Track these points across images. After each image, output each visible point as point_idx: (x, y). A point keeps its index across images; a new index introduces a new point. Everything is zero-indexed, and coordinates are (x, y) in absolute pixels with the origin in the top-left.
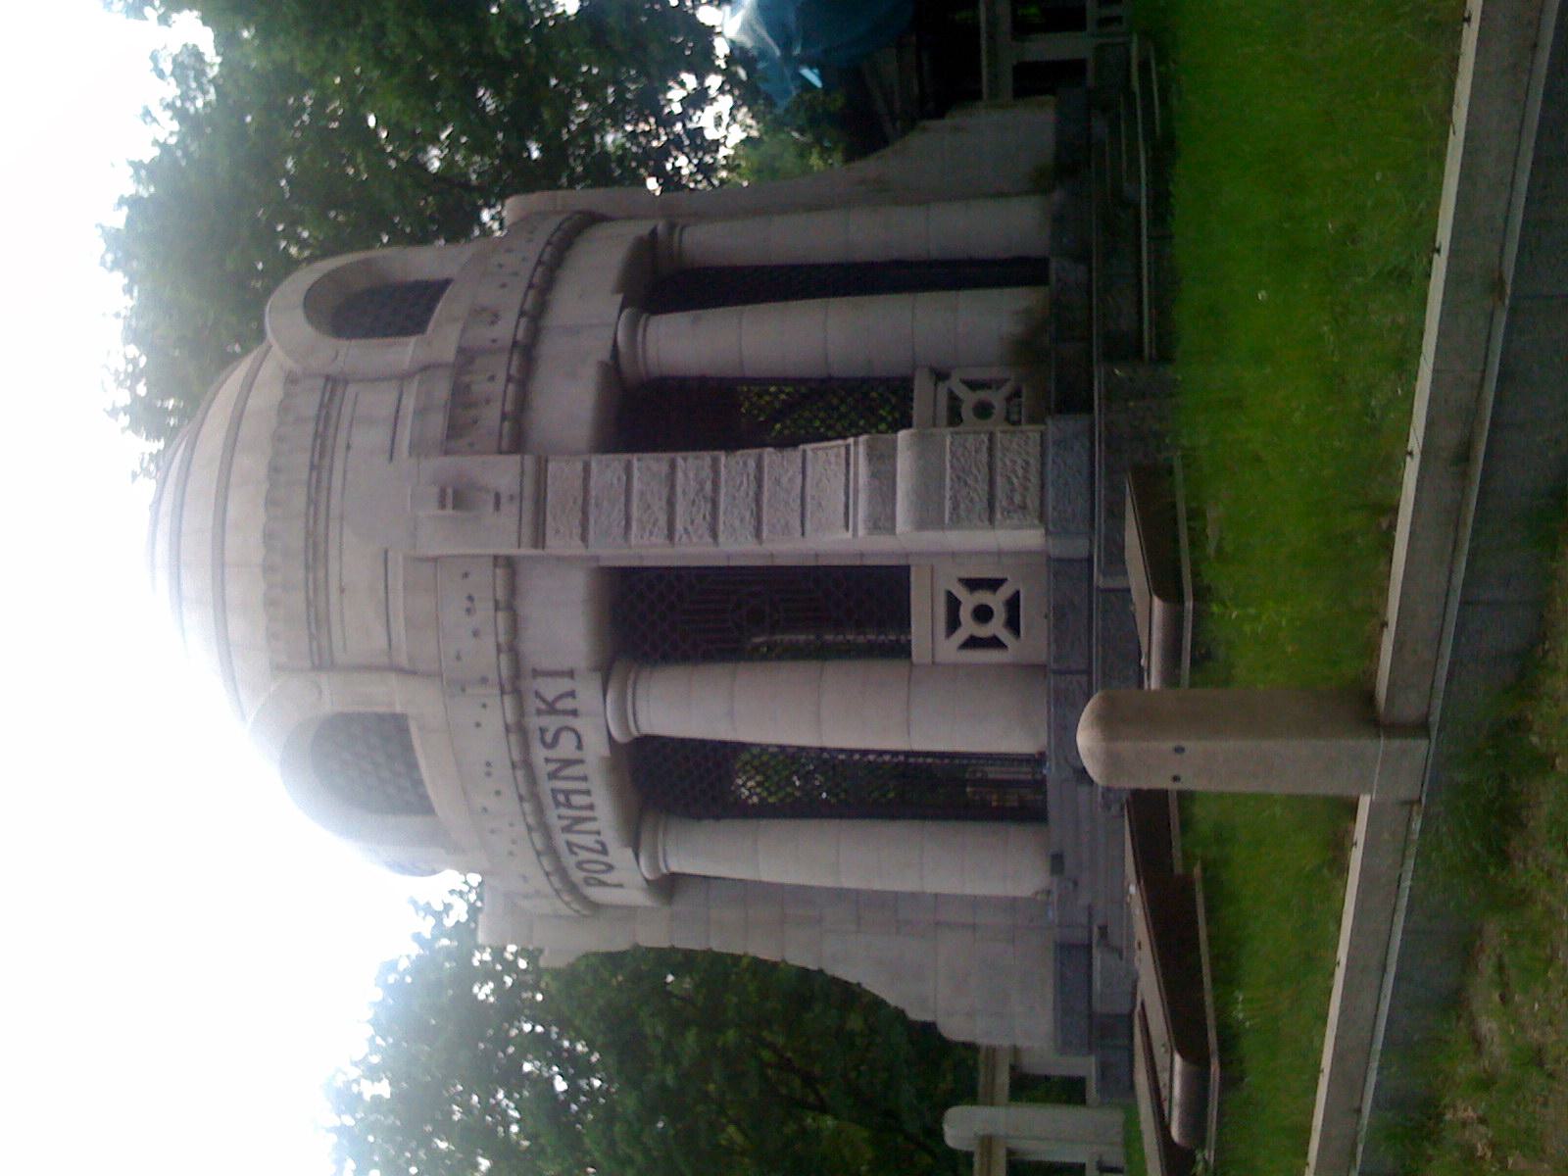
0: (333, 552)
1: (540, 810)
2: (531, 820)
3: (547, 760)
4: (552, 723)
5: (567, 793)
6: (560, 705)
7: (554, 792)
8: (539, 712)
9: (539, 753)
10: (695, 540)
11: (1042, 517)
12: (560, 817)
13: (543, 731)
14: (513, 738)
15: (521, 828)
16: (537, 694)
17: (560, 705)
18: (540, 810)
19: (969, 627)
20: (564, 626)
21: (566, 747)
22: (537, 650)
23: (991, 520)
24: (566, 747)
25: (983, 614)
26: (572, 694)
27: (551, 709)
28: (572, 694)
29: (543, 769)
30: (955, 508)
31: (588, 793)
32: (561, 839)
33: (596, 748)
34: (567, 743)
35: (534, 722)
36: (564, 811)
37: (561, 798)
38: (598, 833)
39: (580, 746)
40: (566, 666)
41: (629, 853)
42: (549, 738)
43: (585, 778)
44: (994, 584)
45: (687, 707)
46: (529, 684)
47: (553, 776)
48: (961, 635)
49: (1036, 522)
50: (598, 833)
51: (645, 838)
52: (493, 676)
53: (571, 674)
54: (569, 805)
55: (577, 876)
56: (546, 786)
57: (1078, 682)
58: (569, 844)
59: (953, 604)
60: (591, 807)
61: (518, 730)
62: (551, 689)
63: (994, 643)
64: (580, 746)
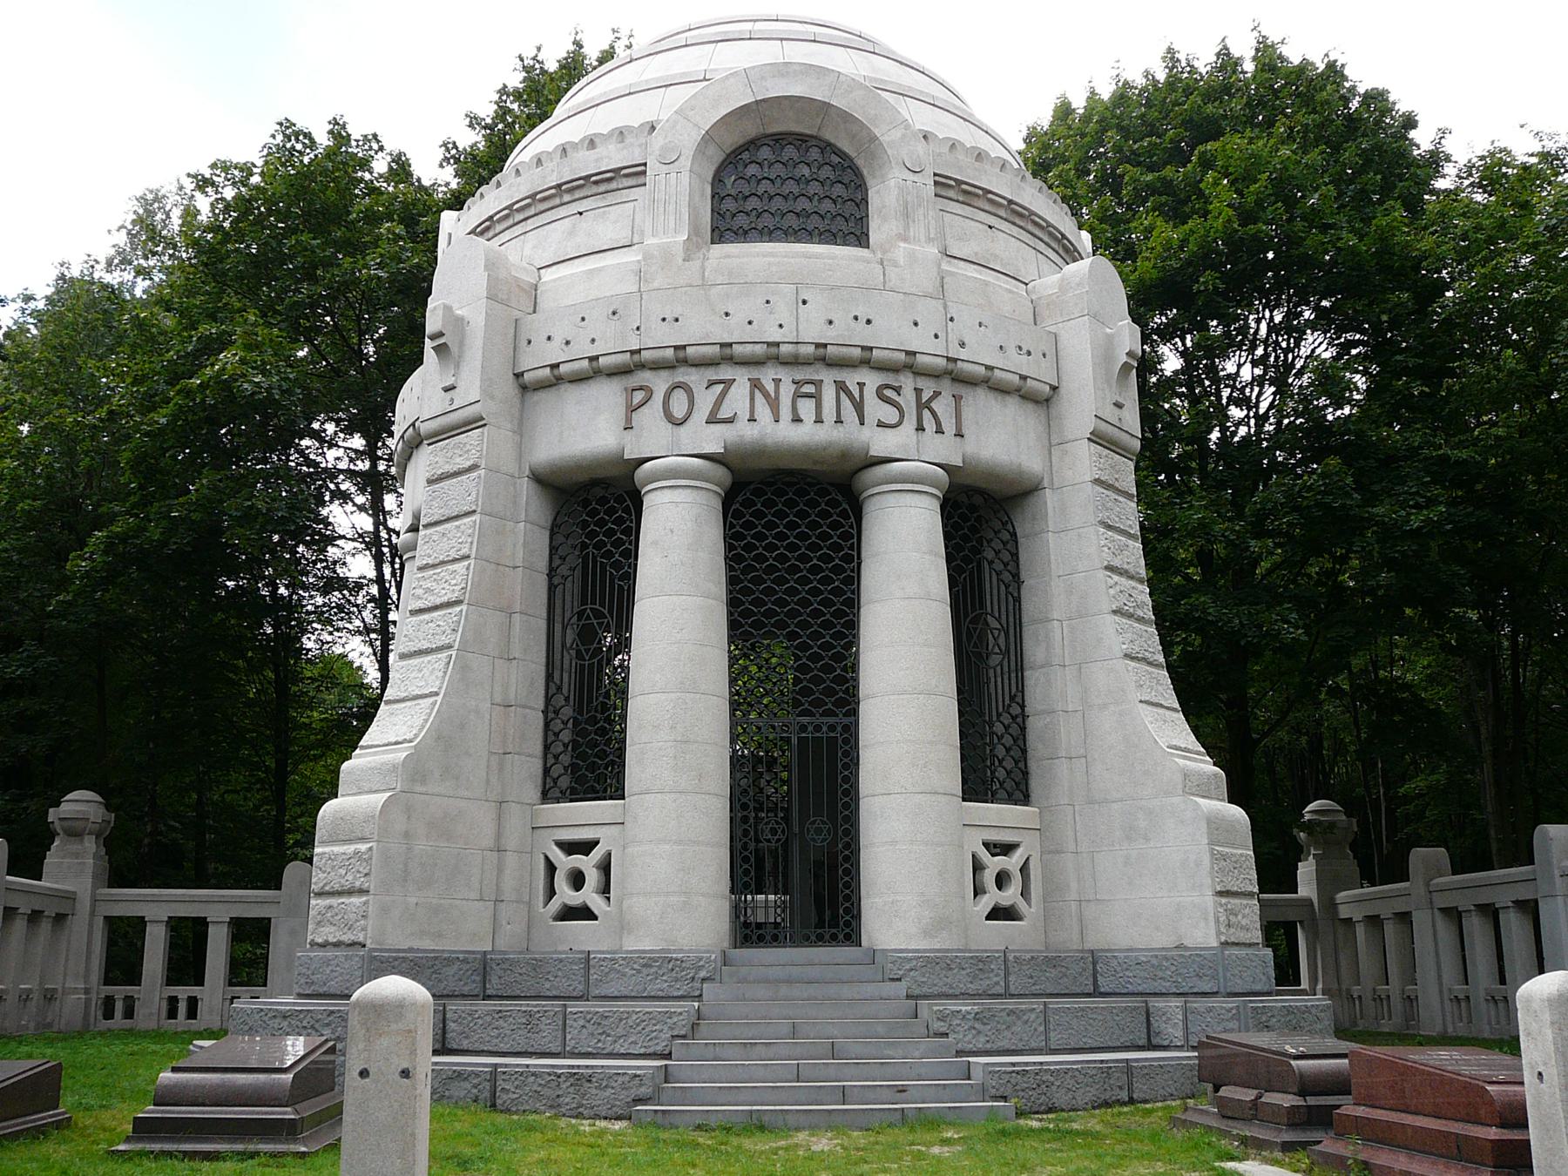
0: (1015, 231)
1: (794, 362)
2: (784, 349)
3: (861, 385)
4: (908, 399)
5: (817, 397)
6: (926, 414)
7: (818, 384)
8: (918, 391)
9: (872, 380)
10: (1112, 591)
11: (1226, 944)
12: (777, 381)
13: (898, 390)
14: (857, 352)
15: (776, 336)
16: (937, 394)
17: (926, 414)
18: (794, 362)
19: (994, 864)
20: (998, 439)
21: (876, 409)
22: (979, 404)
23: (1220, 894)
24: (876, 409)
25: (1002, 880)
26: (940, 431)
27: (922, 406)
28: (940, 431)
29: (852, 379)
30: (1224, 857)
31: (819, 420)
32: (742, 377)
33: (881, 443)
34: (890, 414)
35: (907, 382)
36: (787, 391)
37: (810, 389)
38: (752, 420)
39: (881, 424)
40: (965, 431)
41: (715, 448)
42: (889, 393)
43: (839, 421)
44: (1025, 893)
45: (903, 555)
46: (947, 388)
47: (841, 387)
48: (984, 855)
49: (1223, 939)
50: (752, 420)
51: (720, 472)
52: (963, 354)
53: (959, 435)
54: (798, 395)
55: (660, 383)
56: (828, 377)
57: (997, 983)
58: (728, 383)
59: (1006, 849)
60: (797, 420)
61: (909, 365)
62: (943, 406)
63: (978, 891)
64: (881, 424)
